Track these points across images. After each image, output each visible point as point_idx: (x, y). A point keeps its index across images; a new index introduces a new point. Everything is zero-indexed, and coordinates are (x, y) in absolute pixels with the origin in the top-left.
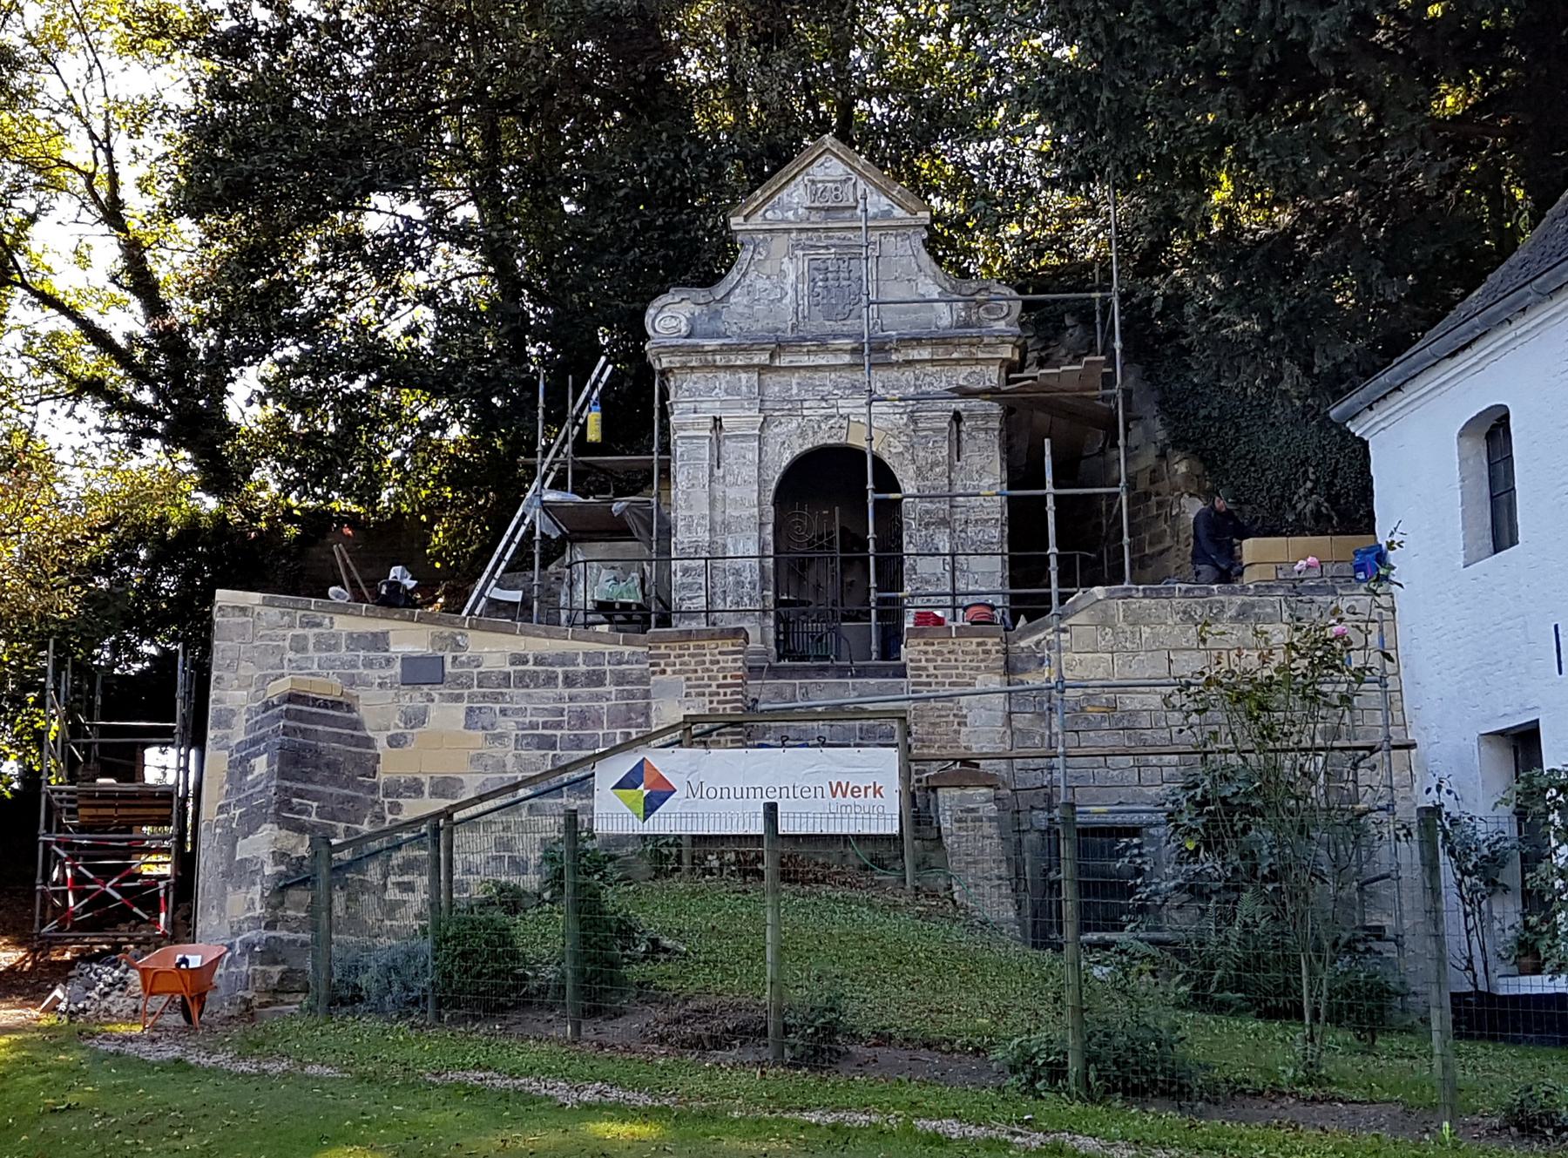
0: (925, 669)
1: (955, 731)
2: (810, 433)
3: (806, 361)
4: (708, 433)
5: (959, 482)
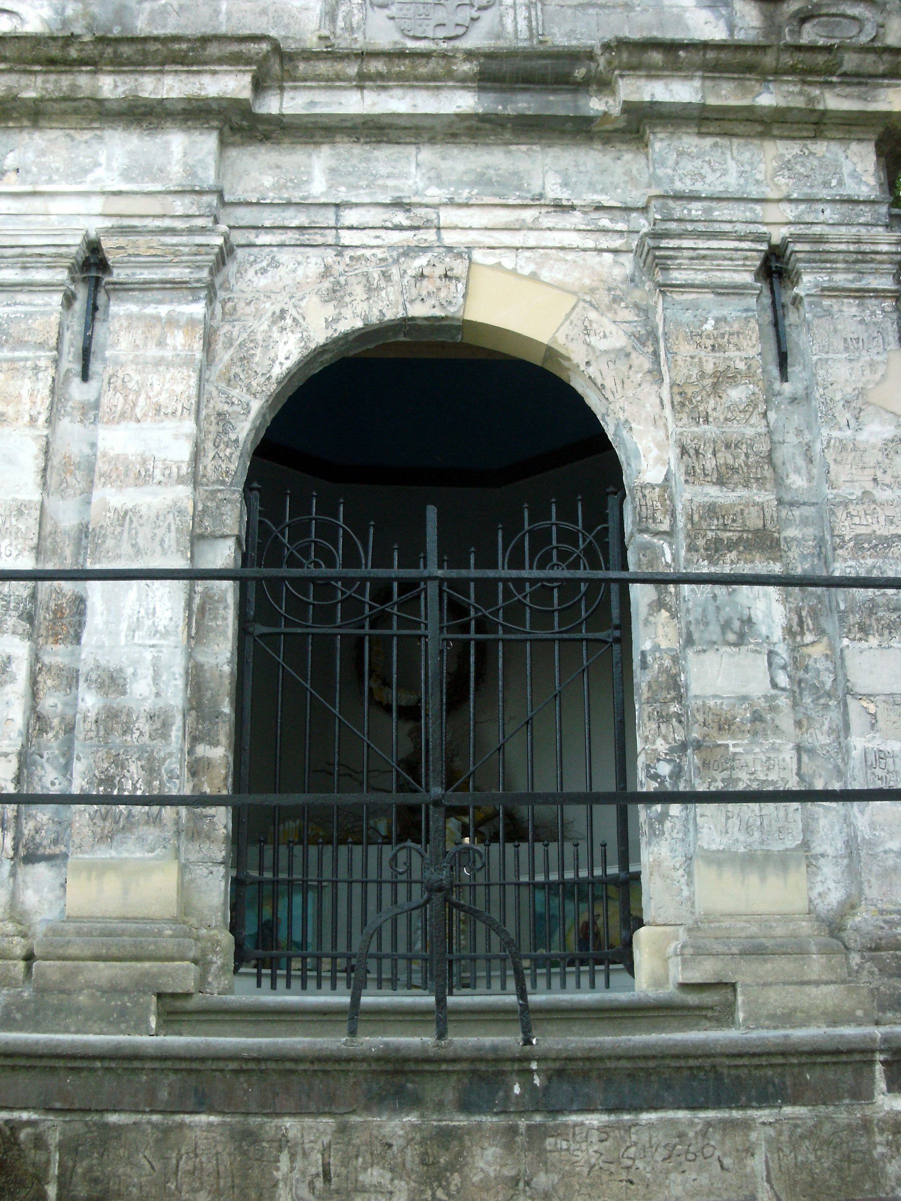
2: (359, 291)
5: (791, 438)
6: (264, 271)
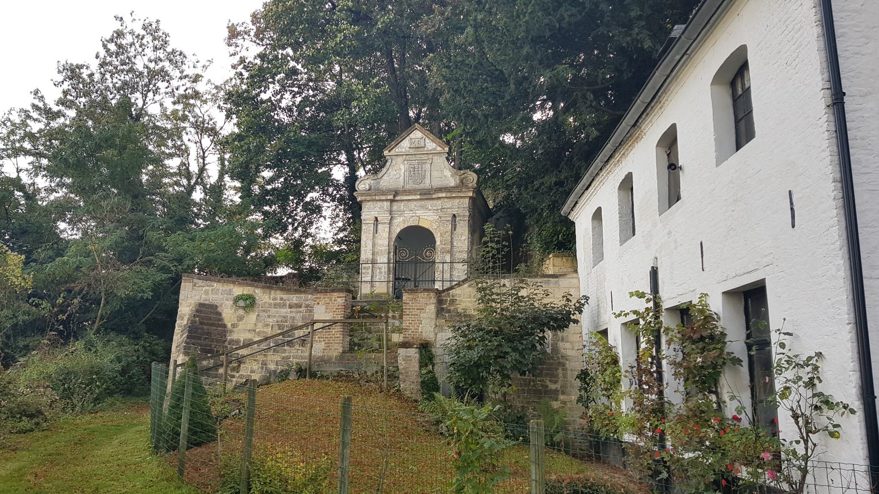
0: (409, 303)
1: (417, 326)
3: (405, 198)
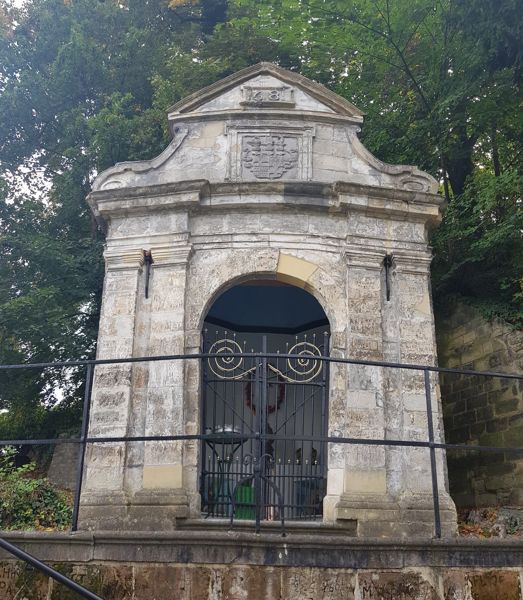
3: (237, 200)
4: (138, 264)
6: (206, 258)
